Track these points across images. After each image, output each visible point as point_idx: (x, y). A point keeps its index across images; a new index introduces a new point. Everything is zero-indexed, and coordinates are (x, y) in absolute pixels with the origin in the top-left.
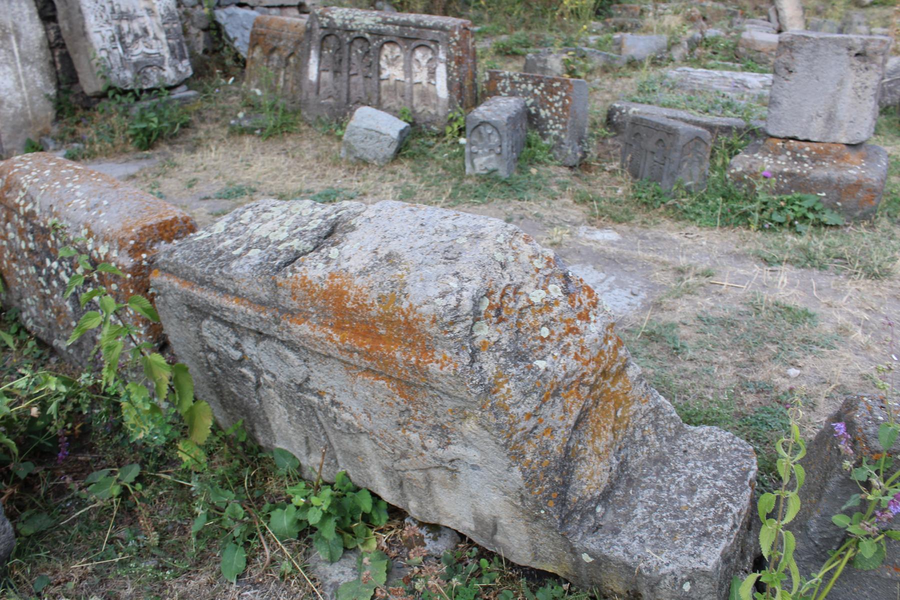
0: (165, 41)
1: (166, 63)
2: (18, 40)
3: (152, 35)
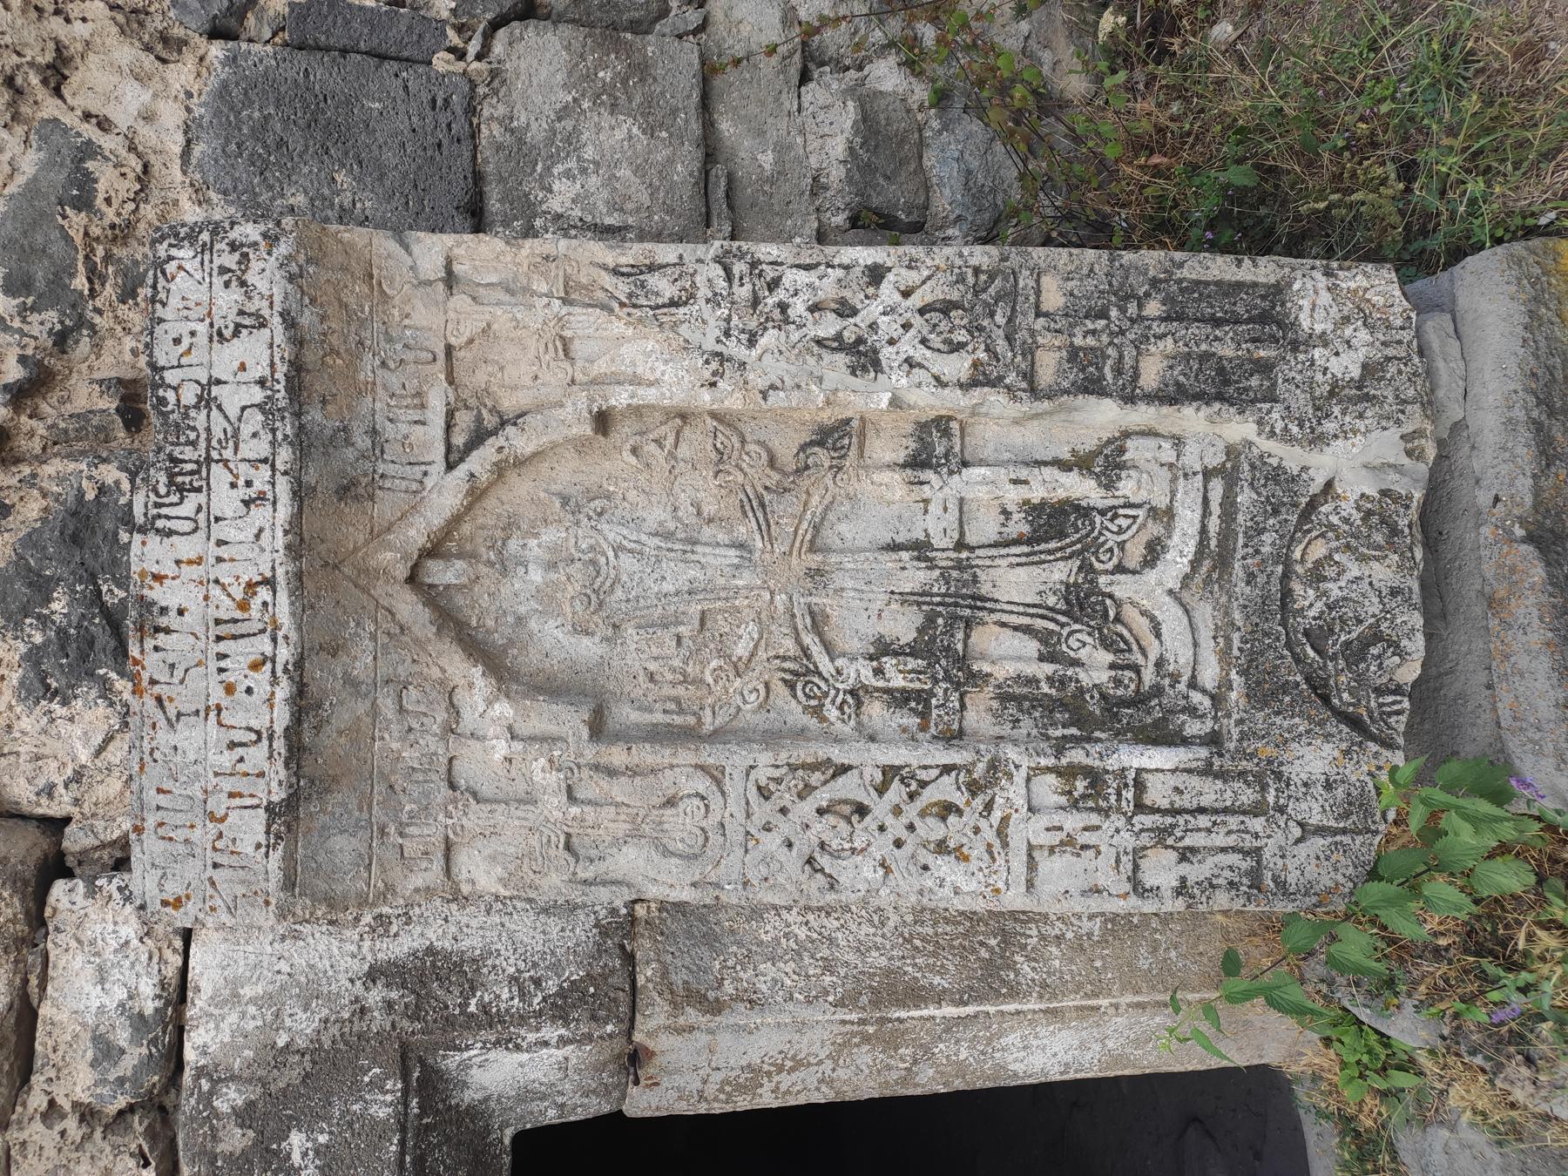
0: (1143, 415)
1: (1291, 457)
2: (916, 995)
3: (1081, 488)
